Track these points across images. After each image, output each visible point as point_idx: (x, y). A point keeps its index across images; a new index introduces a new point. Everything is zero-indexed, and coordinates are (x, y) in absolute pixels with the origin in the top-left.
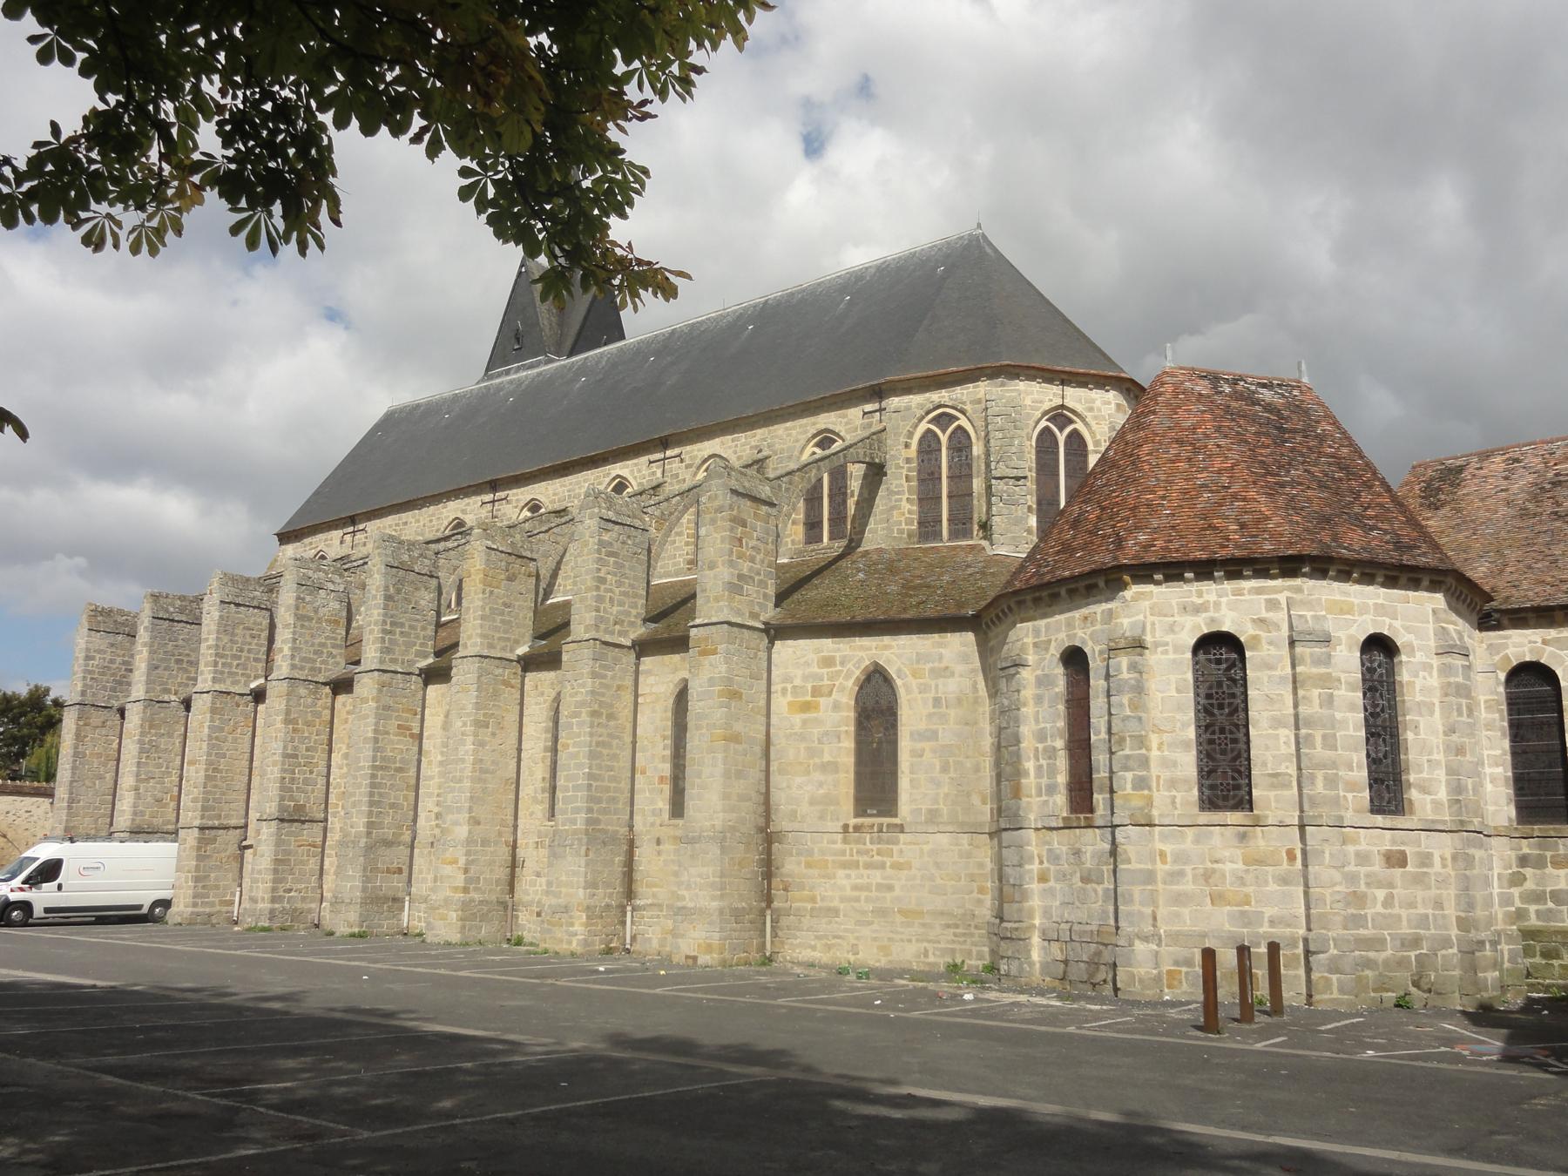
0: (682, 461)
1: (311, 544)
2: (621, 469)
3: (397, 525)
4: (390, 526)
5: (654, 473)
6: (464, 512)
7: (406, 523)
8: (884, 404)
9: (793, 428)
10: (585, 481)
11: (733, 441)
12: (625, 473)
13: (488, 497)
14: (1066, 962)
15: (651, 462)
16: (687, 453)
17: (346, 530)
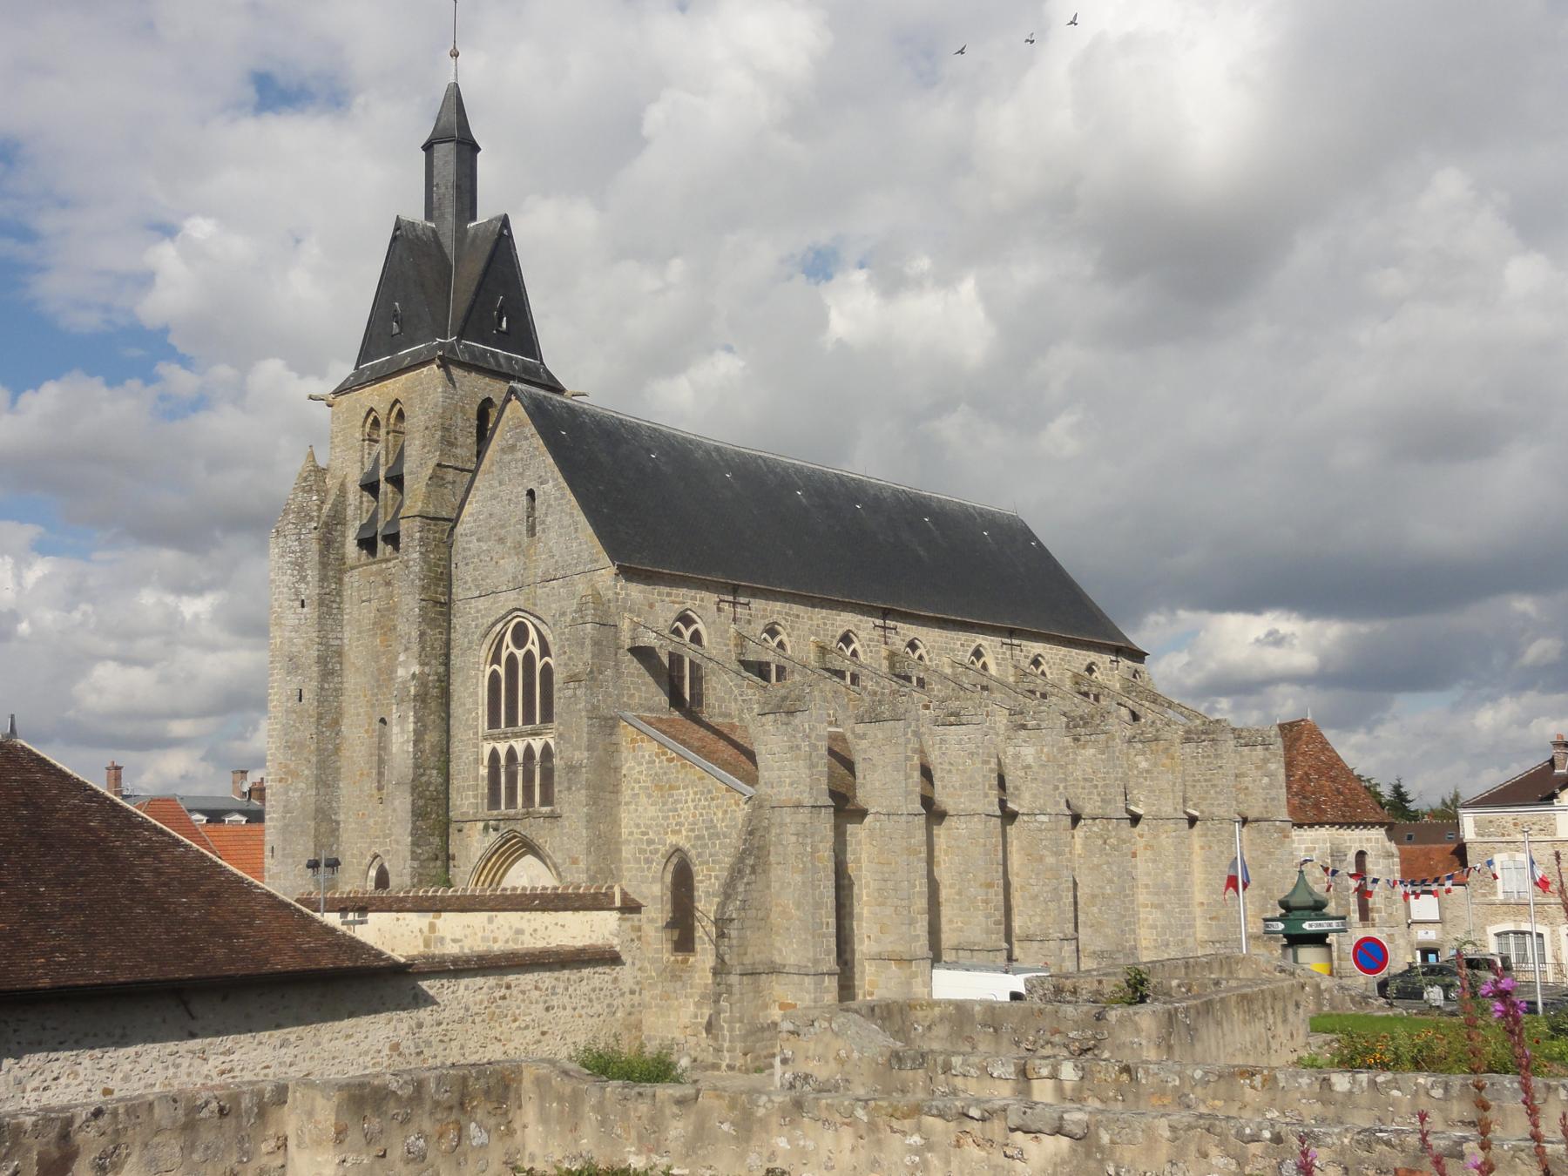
0: (1021, 651)
1: (678, 595)
2: (984, 639)
3: (787, 614)
4: (779, 613)
5: (1004, 653)
6: (857, 627)
7: (798, 616)
8: (1119, 659)
9: (1079, 654)
10: (958, 639)
11: (1050, 649)
12: (984, 643)
13: (879, 622)
14: (1366, 984)
15: (1003, 644)
16: (1025, 646)
17: (722, 597)
